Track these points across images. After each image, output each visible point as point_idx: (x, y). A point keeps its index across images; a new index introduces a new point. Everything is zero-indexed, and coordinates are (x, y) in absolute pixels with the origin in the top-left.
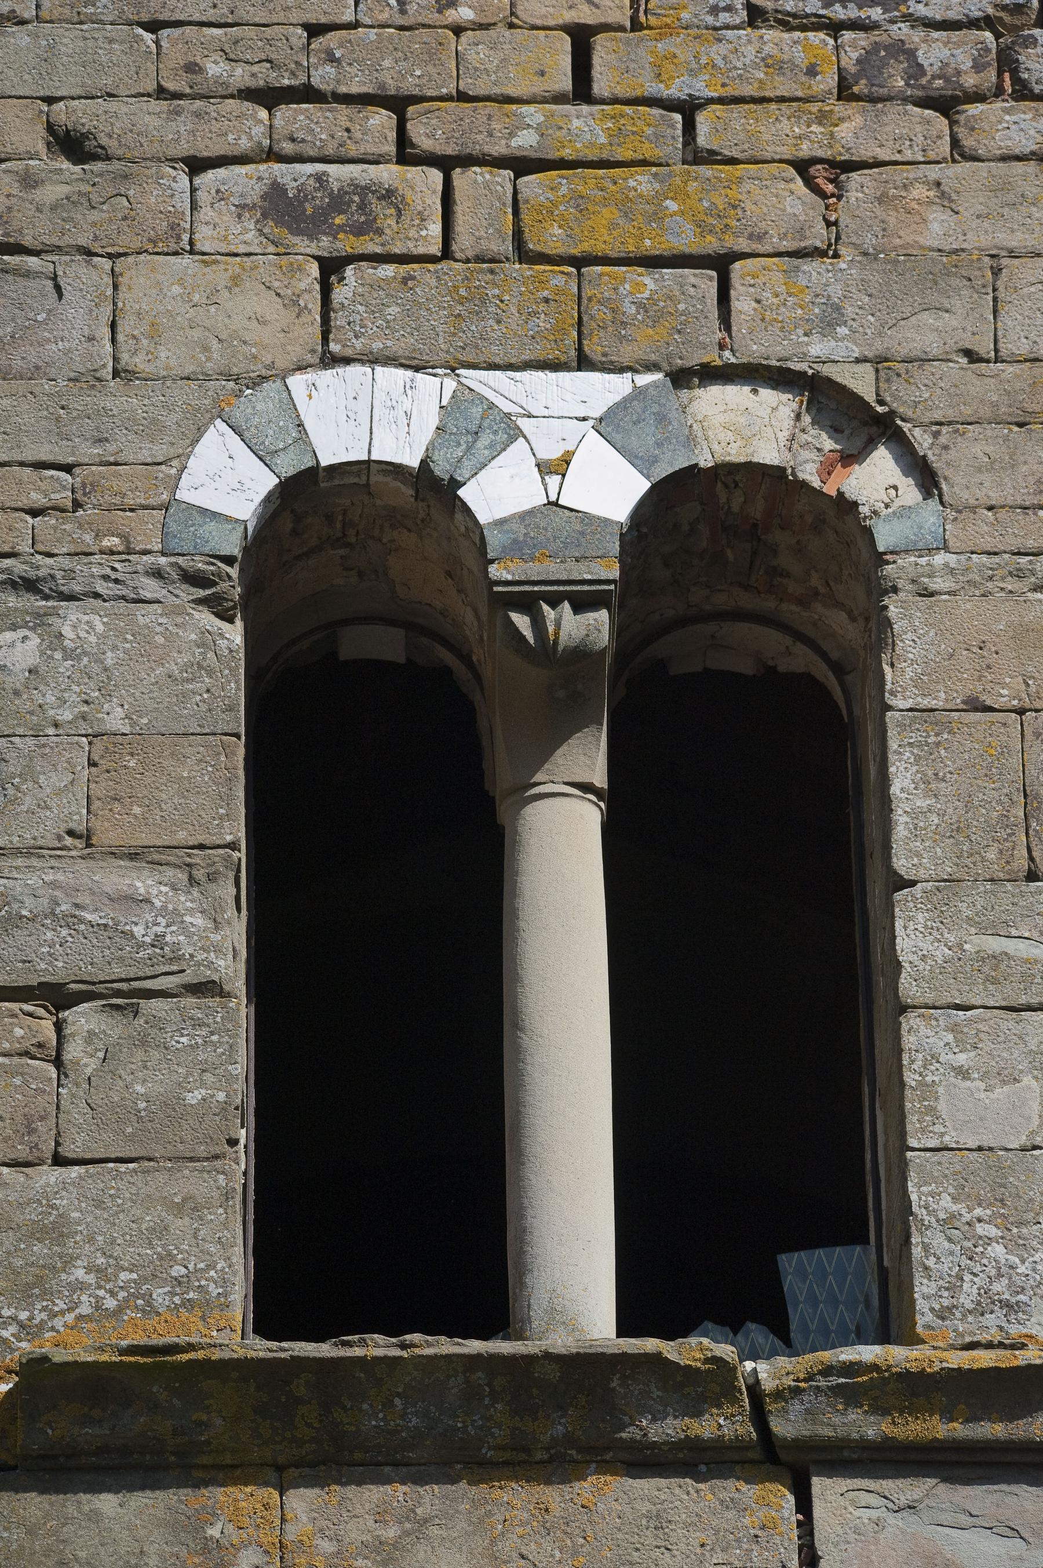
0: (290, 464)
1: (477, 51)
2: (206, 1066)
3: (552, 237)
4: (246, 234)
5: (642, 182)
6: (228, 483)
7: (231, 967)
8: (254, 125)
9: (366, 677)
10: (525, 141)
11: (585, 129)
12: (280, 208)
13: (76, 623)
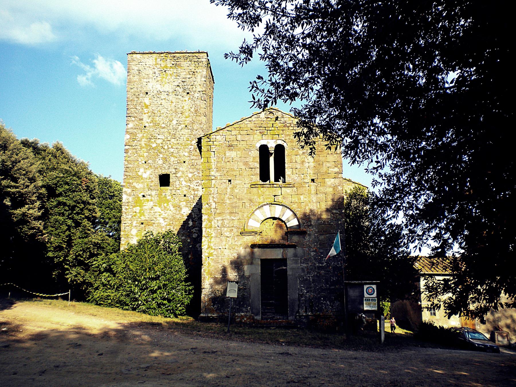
6: (258, 146)
8: (259, 128)
9: (264, 150)
11: (273, 129)
12: (260, 132)
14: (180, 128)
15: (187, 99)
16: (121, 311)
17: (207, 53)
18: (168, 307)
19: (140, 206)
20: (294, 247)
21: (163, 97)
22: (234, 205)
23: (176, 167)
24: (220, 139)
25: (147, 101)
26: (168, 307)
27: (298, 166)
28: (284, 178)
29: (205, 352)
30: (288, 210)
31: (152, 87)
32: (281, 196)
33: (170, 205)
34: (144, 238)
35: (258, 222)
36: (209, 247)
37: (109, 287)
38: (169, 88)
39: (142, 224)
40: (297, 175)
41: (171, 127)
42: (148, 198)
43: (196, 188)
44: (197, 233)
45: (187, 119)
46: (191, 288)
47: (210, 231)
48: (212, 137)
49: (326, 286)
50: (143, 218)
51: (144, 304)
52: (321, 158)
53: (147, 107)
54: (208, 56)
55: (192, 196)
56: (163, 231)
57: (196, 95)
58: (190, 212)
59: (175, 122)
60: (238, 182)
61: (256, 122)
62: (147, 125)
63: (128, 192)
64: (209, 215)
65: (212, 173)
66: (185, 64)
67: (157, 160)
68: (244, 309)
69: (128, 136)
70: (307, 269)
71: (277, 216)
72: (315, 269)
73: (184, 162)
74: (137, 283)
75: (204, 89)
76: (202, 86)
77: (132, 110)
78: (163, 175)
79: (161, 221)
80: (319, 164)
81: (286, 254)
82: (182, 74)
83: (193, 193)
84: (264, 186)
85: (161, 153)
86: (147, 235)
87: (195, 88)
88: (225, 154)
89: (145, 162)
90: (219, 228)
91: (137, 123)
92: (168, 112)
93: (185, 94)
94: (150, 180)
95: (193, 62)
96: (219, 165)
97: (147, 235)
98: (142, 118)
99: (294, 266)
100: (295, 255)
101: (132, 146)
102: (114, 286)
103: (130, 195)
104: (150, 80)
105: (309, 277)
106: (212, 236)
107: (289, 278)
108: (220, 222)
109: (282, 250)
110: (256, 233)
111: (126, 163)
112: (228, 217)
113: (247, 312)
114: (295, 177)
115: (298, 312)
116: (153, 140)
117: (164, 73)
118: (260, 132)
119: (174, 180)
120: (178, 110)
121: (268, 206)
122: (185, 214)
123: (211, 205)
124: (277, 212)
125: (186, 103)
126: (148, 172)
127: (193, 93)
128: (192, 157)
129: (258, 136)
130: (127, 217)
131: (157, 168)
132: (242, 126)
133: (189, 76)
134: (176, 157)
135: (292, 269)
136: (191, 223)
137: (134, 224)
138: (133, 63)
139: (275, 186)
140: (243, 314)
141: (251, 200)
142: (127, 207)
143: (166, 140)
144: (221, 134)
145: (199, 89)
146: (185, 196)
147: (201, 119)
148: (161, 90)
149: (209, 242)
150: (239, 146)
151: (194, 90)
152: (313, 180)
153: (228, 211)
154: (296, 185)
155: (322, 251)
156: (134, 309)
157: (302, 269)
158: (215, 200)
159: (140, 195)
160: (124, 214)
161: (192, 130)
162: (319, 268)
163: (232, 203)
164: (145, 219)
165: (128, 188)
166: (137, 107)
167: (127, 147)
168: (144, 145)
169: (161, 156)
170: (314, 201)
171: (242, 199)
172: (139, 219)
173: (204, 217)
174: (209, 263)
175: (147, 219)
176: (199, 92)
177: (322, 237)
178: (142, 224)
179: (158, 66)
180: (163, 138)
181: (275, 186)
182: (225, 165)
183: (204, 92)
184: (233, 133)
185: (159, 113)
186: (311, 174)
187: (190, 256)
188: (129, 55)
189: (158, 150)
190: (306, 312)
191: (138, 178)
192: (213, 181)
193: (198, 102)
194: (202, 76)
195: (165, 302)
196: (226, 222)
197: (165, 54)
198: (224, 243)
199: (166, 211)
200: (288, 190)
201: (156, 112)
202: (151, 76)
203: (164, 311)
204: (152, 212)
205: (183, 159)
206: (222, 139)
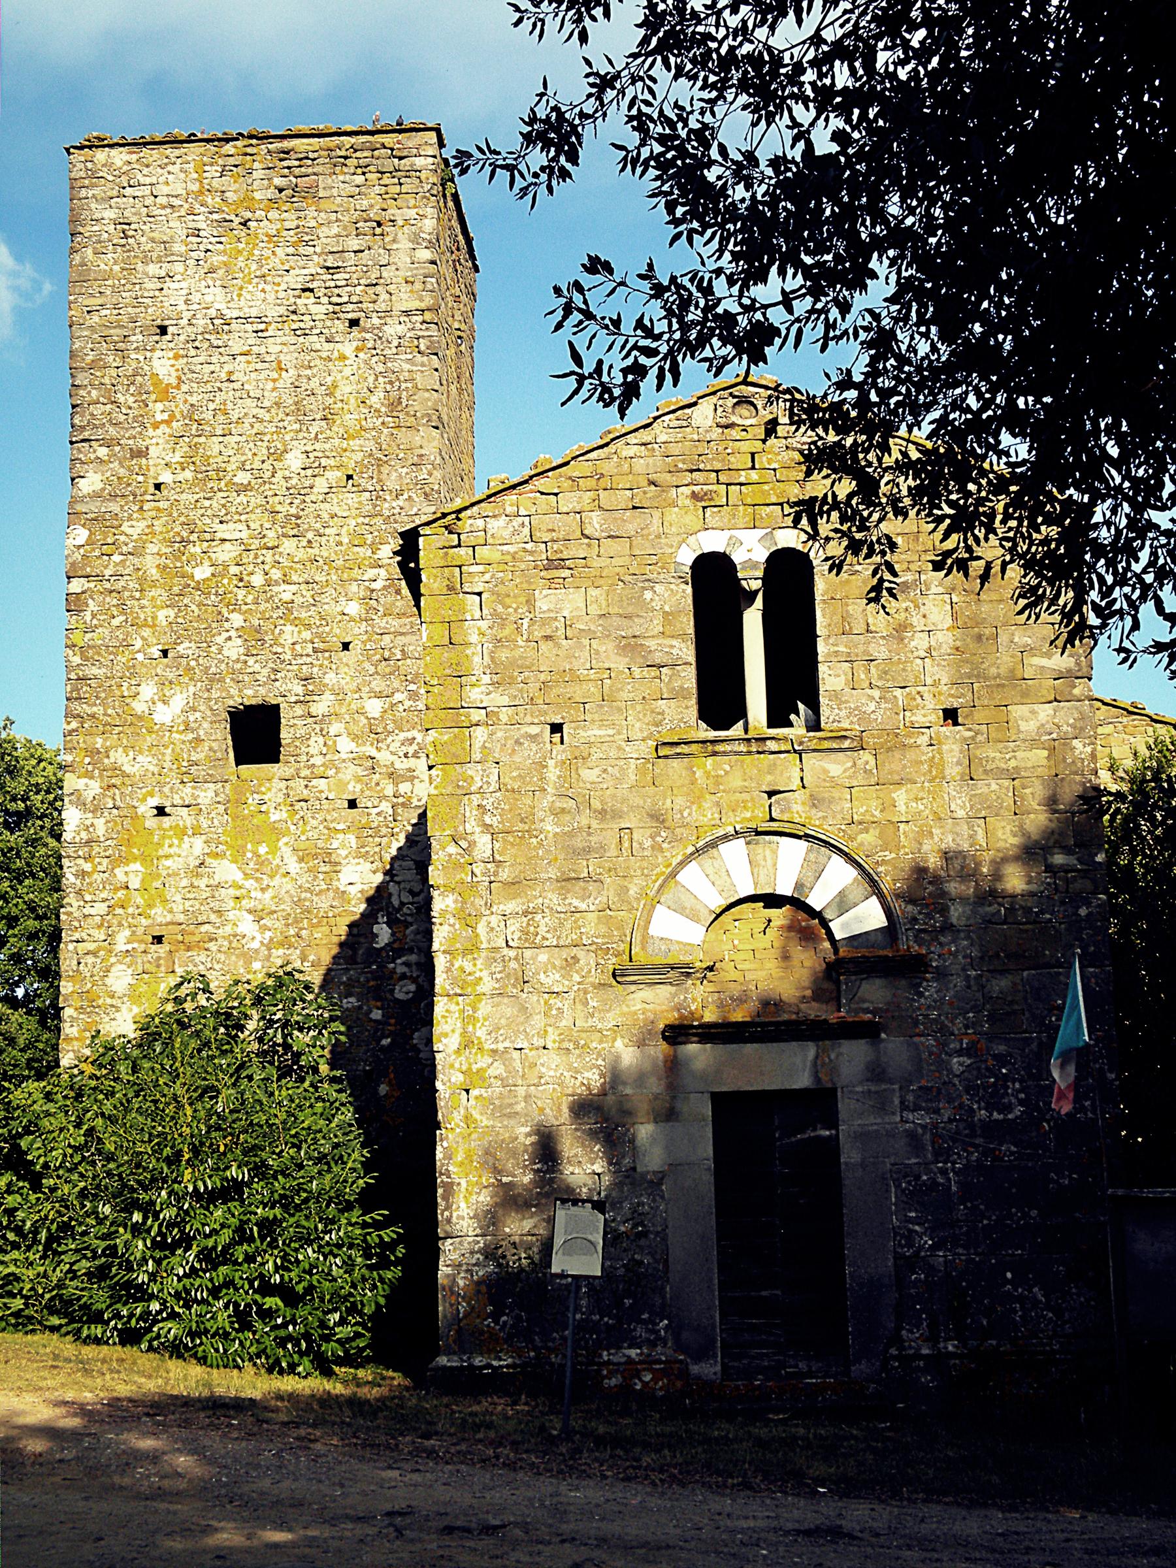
0: (699, 552)
1: (732, 459)
2: (689, 678)
3: (749, 501)
4: (688, 502)
5: (766, 487)
6: (687, 557)
7: (692, 659)
8: (688, 478)
9: (713, 577)
10: (742, 480)
11: (754, 476)
12: (694, 496)
13: (658, 587)
14: (321, 485)
15: (348, 349)
16: (68, 1347)
17: (438, 131)
18: (285, 1325)
19: (144, 859)
20: (867, 1031)
21: (237, 347)
22: (578, 842)
24: (506, 533)
25: (163, 365)
26: (285, 1325)
27: (880, 651)
28: (814, 706)
29: (449, 1530)
30: (837, 860)
32: (800, 795)
33: (286, 851)
34: (169, 1007)
35: (694, 917)
36: (467, 1043)
37: (11, 1236)
38: (262, 300)
39: (158, 939)
40: (876, 693)
43: (401, 765)
44: (414, 980)
45: (355, 444)
46: (388, 1235)
47: (468, 967)
48: (468, 523)
49: (1026, 1215)
50: (160, 914)
51: (174, 1316)
52: (985, 608)
53: (165, 394)
54: (441, 144)
55: (386, 807)
56: (258, 973)
57: (393, 329)
58: (379, 878)
59: (294, 460)
60: (594, 732)
61: (675, 449)
62: (166, 477)
63: (89, 795)
64: (463, 890)
65: (475, 695)
66: (337, 185)
67: (219, 639)
68: (640, 1331)
69: (81, 535)
70: (935, 1136)
71: (785, 889)
72: (973, 1135)
73: (346, 646)
74: (137, 1217)
75: (428, 301)
76: (418, 286)
77: (98, 410)
78: (249, 708)
79: (247, 925)
80: (979, 638)
81: (834, 1070)
82: (323, 232)
83: (389, 790)
84: (719, 748)
85: (234, 606)
86: (183, 992)
88: (530, 602)
89: (165, 653)
90: (512, 953)
91: (122, 472)
92: (261, 413)
93: (341, 326)
94: (191, 736)
95: (373, 177)
96: (503, 655)
97: (183, 992)
98: (142, 444)
99: (872, 1122)
100: (876, 1072)
101: (100, 578)
102: (35, 1231)
105: (944, 1172)
106: (480, 989)
107: (850, 1180)
108: (514, 926)
109: (811, 1050)
110: (684, 971)
111: (77, 660)
112: (553, 899)
113: (652, 1344)
114: (869, 703)
115: (898, 1341)
116: (196, 550)
118: (694, 496)
119: (301, 732)
120: (311, 404)
121: (741, 842)
122: (353, 890)
123: (472, 844)
124: (786, 863)
125: (348, 371)
126: (179, 701)
127: (376, 321)
128: (381, 623)
129: (681, 512)
130: (86, 911)
131: (215, 679)
132: (607, 468)
133: (354, 243)
134: (308, 626)
135: (863, 1137)
136: (383, 933)
138: (96, 191)
139: (771, 745)
140: (633, 1353)
141: (658, 818)
142: (87, 867)
144: (509, 510)
145: (406, 300)
146: (352, 804)
147: (417, 440)
148: (229, 314)
149: (468, 1019)
150: (596, 563)
152: (950, 715)
153: (553, 873)
154: (870, 741)
155: (1001, 1048)
156: (130, 1337)
157: (912, 1135)
158: (488, 820)
159: (146, 809)
160: (71, 899)
161: (377, 496)
162: (989, 1128)
163: (570, 835)
164: (169, 918)
166: (122, 399)
167: (76, 586)
168: (154, 573)
169: (237, 620)
170: (961, 813)
171: (617, 815)
172: (145, 922)
173: (441, 903)
174: (468, 1118)
175: (181, 918)
176: (406, 313)
177: (1000, 985)
178: (158, 939)
179: (212, 201)
180: (245, 535)
181: (771, 745)
182: (531, 654)
183: (428, 316)
184: (568, 502)
185: (221, 418)
186: (938, 682)
187: (383, 1089)
188: (78, 156)
189: (218, 597)
190: (932, 1338)
191: (135, 726)
192: (480, 734)
193: (402, 364)
194: (415, 239)
195: (272, 1302)
196: (544, 923)
197: (239, 144)
198: (538, 1021)
199: (266, 880)
200: (836, 766)
201: (208, 415)
202: (179, 248)
203: (269, 1342)
204: (202, 883)
206: (515, 532)
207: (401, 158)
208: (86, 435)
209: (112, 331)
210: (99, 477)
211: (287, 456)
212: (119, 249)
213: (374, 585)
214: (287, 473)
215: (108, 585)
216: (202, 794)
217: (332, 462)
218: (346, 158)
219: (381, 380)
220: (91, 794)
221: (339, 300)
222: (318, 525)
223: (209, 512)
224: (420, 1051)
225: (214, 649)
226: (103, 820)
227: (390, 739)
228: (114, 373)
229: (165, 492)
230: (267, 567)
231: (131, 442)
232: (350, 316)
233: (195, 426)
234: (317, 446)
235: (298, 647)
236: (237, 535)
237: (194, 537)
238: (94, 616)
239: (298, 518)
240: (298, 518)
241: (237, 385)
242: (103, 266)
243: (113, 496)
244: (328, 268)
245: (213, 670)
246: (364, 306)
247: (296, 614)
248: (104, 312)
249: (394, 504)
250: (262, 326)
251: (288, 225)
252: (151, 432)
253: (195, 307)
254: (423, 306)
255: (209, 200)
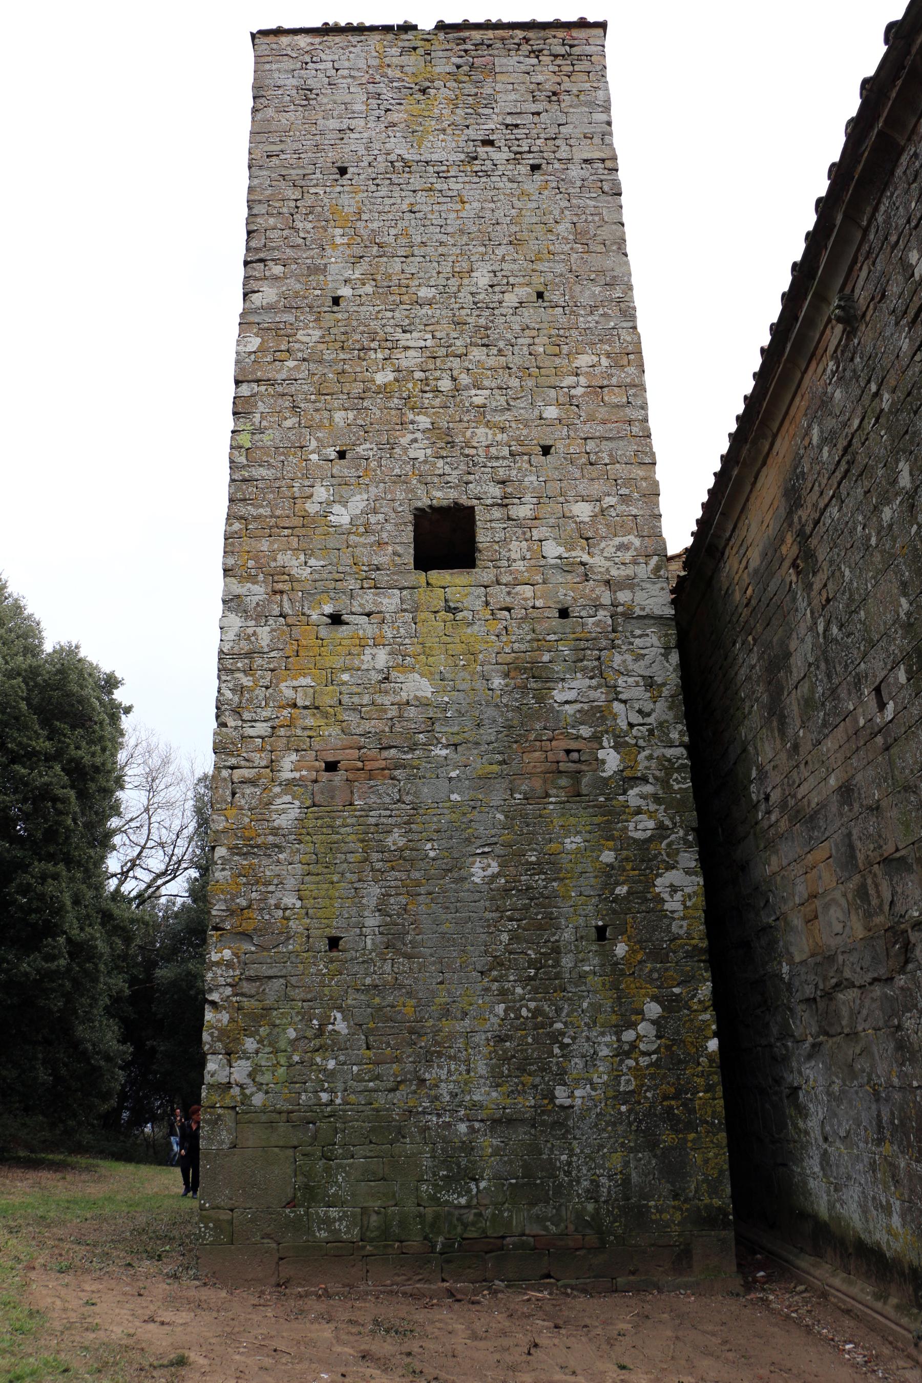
14: (511, 299)
23: (501, 472)
31: (368, 149)
39: (331, 767)
41: (465, 297)
42: (365, 627)
44: (651, 815)
59: (482, 278)
62: (345, 292)
67: (405, 441)
76: (597, 140)
83: (606, 599)
85: (422, 409)
87: (564, 147)
92: (444, 238)
93: (524, 169)
94: (373, 538)
95: (546, 59)
103: (261, 616)
104: (359, 123)
111: (243, 460)
117: (419, 96)
119: (500, 535)
126: (358, 503)
128: (587, 429)
133: (534, 108)
134: (503, 430)
137: (288, 766)
142: (246, 681)
143: (442, 352)
151: (563, 153)
165: (252, 579)
166: (299, 225)
169: (424, 421)
176: (585, 161)
178: (331, 767)
185: (403, 241)
187: (621, 949)
189: (407, 397)
191: (305, 528)
204: (386, 700)
205: (539, 436)
207: (571, 46)
208: (262, 255)
209: (292, 172)
210: (275, 291)
211: (473, 274)
212: (300, 109)
213: (573, 392)
214: (474, 290)
215: (280, 389)
216: (385, 601)
217: (521, 280)
218: (519, 45)
219: (567, 212)
220: (255, 599)
221: (520, 149)
222: (509, 336)
223: (392, 322)
224: (663, 901)
225: (397, 450)
226: (267, 628)
227: (603, 545)
228: (292, 204)
229: (343, 304)
230: (455, 373)
231: (309, 261)
232: (531, 162)
233: (376, 248)
234: (505, 266)
235: (493, 450)
236: (422, 344)
237: (374, 345)
238: (262, 418)
239: (487, 329)
240: (487, 329)
241: (418, 215)
242: (284, 121)
243: (288, 308)
244: (507, 126)
245: (397, 471)
246: (545, 154)
247: (488, 417)
248: (283, 156)
249: (590, 319)
250: (444, 168)
251: (466, 91)
252: (329, 252)
253: (376, 152)
254: (603, 156)
255: (389, 72)
